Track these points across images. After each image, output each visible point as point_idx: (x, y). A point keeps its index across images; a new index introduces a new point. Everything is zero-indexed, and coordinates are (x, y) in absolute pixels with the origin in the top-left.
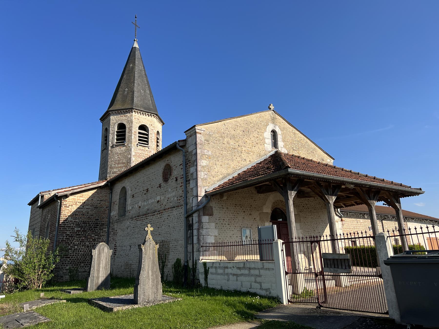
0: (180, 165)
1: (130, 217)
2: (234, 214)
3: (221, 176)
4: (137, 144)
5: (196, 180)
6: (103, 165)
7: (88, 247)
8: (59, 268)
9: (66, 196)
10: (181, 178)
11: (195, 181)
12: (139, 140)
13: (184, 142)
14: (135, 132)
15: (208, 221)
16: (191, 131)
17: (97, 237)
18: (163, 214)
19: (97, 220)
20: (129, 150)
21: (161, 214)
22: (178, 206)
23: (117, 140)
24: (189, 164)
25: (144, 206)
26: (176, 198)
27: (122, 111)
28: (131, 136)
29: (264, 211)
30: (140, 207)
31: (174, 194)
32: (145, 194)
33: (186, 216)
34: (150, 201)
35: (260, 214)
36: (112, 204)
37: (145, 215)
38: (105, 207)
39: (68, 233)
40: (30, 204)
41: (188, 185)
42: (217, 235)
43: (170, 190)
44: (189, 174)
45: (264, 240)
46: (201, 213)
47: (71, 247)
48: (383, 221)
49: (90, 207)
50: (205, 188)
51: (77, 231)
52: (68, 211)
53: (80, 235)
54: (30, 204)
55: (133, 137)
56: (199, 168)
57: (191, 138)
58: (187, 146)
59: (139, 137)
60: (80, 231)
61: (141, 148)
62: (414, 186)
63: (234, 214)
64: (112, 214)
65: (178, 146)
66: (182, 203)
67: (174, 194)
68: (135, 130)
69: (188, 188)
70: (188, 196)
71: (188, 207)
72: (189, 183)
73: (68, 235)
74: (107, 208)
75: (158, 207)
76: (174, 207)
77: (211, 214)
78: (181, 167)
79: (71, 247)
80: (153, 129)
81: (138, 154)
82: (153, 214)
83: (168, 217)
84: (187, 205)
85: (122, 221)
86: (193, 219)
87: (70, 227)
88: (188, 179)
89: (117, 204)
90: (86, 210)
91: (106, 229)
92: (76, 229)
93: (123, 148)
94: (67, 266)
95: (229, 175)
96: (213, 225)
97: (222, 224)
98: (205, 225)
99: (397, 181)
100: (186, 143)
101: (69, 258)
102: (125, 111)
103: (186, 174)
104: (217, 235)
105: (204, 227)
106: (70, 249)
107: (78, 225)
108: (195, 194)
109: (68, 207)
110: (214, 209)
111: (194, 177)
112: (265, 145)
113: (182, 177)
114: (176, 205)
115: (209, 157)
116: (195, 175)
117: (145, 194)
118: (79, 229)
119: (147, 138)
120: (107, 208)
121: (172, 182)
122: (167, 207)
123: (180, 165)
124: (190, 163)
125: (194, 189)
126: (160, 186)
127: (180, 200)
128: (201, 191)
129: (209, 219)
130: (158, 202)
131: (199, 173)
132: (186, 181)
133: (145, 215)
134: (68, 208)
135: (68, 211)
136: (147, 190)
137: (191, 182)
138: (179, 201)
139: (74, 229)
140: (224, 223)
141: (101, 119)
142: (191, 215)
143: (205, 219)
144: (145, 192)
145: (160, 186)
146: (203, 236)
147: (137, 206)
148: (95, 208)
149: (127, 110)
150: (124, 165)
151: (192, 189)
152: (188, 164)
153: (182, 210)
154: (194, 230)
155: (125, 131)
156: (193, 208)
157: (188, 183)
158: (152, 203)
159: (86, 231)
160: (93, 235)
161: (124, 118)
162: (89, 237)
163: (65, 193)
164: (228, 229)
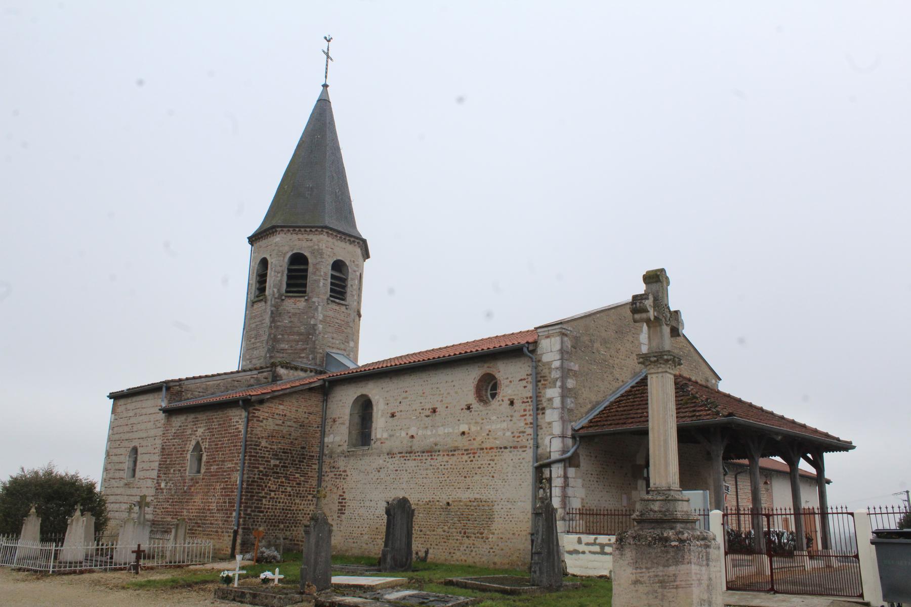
0: (521, 380)
1: (385, 451)
3: (589, 406)
4: (328, 299)
6: (253, 333)
7: (290, 496)
8: (249, 529)
9: (261, 402)
10: (523, 402)
12: (332, 290)
14: (326, 274)
17: (302, 479)
18: (476, 456)
19: (303, 448)
21: (472, 455)
22: (515, 447)
23: (288, 285)
24: (543, 382)
26: (508, 434)
28: (318, 281)
30: (412, 437)
31: (504, 425)
32: (427, 416)
34: (441, 431)
36: (329, 421)
39: (261, 469)
41: (539, 417)
42: (584, 497)
43: (494, 418)
44: (544, 400)
46: (567, 465)
49: (294, 425)
51: (275, 465)
53: (278, 473)
55: (321, 284)
57: (548, 340)
58: (539, 352)
59: (332, 284)
61: (334, 306)
62: (843, 437)
64: (326, 440)
65: (525, 350)
67: (504, 425)
68: (326, 269)
71: (540, 451)
72: (543, 413)
75: (462, 442)
76: (506, 448)
77: (577, 466)
78: (524, 383)
84: (537, 447)
85: (363, 455)
88: (540, 407)
89: (343, 424)
90: (287, 429)
91: (316, 467)
92: (273, 462)
93: (301, 304)
94: (260, 526)
95: (598, 403)
98: (571, 482)
99: (811, 423)
101: (262, 512)
104: (584, 497)
106: (263, 497)
114: (511, 445)
117: (427, 416)
118: (277, 462)
119: (344, 287)
121: (499, 405)
122: (484, 446)
123: (521, 380)
126: (469, 408)
130: (463, 433)
132: (538, 409)
137: (548, 412)
143: (571, 471)
144: (428, 413)
147: (403, 434)
150: (301, 337)
151: (549, 423)
152: (540, 381)
153: (529, 455)
154: (553, 489)
157: (540, 412)
158: (449, 434)
160: (297, 475)
161: (305, 244)
163: (262, 397)
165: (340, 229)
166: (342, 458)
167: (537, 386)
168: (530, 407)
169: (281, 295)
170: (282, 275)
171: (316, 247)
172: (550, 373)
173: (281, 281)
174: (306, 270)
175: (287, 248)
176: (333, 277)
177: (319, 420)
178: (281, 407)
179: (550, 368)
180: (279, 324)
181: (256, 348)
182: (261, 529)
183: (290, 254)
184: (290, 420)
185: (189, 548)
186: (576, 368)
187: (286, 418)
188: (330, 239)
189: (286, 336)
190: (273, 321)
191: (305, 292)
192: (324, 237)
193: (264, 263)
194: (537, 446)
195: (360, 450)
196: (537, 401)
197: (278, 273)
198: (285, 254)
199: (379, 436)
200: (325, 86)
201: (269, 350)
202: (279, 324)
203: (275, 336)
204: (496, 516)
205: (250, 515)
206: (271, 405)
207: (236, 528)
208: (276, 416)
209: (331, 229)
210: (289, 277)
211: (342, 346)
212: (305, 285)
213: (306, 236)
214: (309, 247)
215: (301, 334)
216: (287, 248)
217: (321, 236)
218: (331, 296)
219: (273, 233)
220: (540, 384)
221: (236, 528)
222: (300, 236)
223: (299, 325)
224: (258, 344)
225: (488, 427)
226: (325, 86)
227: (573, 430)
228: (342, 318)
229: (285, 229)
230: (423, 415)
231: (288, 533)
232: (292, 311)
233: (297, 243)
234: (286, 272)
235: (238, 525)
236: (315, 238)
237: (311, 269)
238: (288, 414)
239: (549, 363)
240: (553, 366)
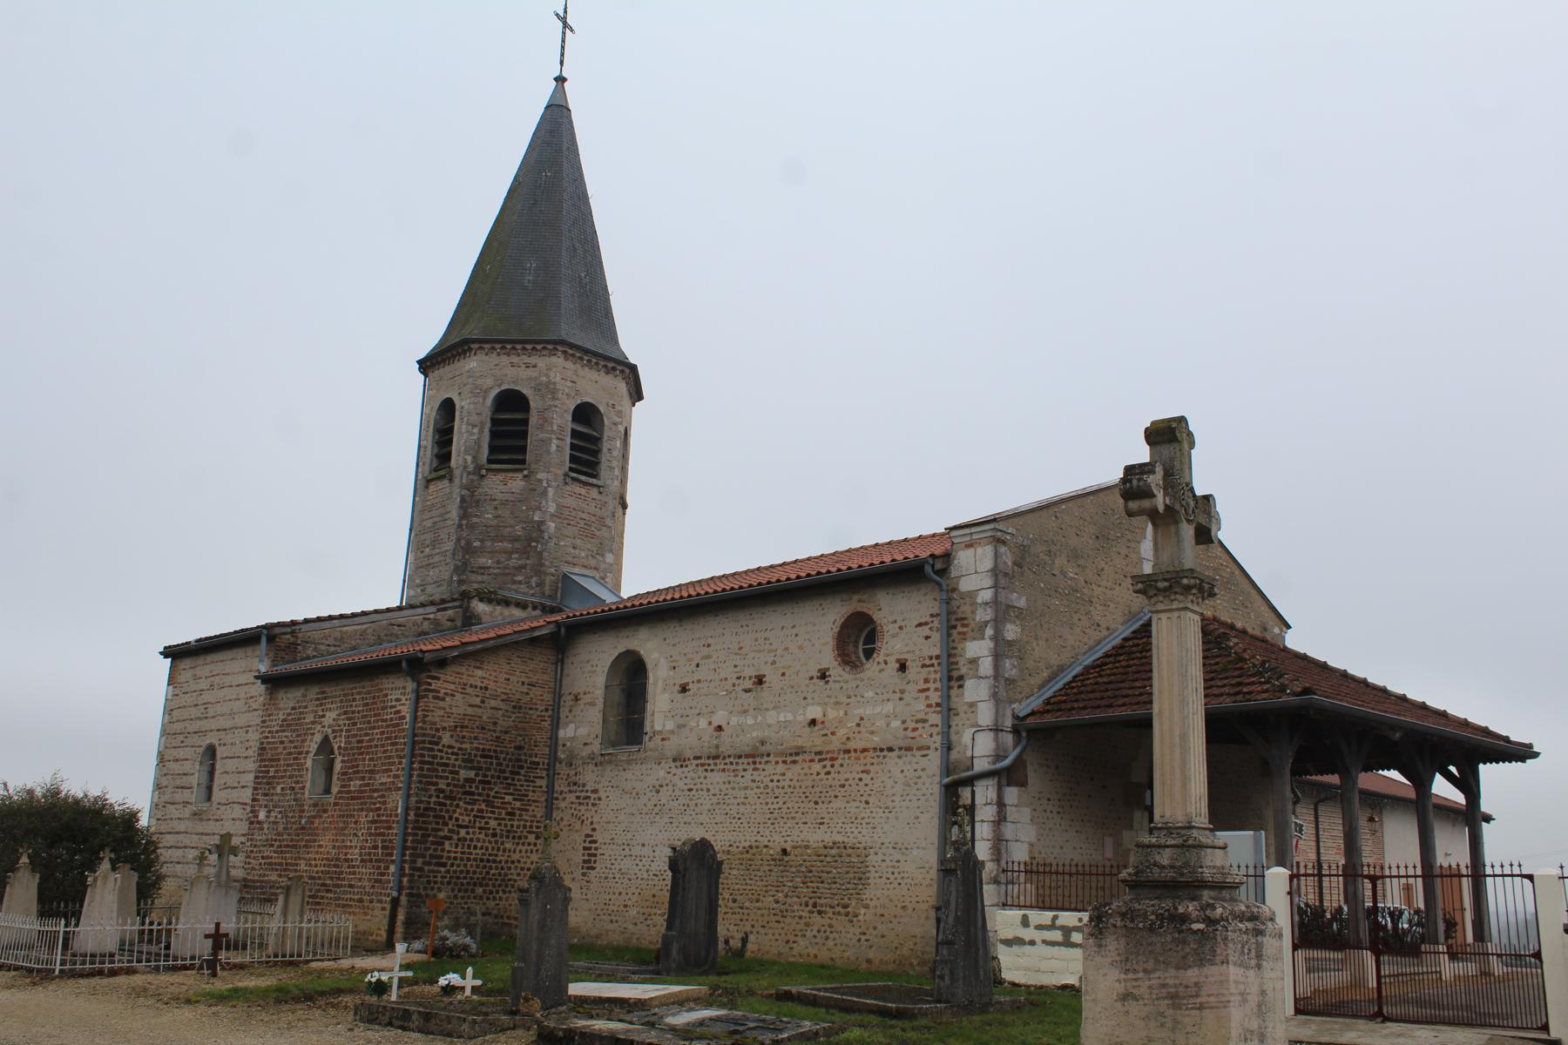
0: (920, 625)
1: (669, 754)
3: (1045, 674)
4: (566, 475)
6: (429, 537)
7: (494, 835)
8: (419, 895)
9: (442, 663)
10: (924, 666)
12: (573, 459)
16: (973, 530)
17: (518, 804)
18: (837, 763)
19: (520, 748)
20: (535, 491)
21: (828, 763)
22: (908, 749)
23: (492, 449)
24: (960, 629)
25: (742, 729)
26: (896, 724)
27: (519, 347)
28: (547, 442)
30: (720, 728)
31: (889, 707)
32: (747, 691)
34: (772, 718)
36: (567, 700)
37: (753, 756)
39: (442, 785)
40: (168, 652)
41: (953, 692)
42: (1034, 840)
43: (871, 694)
44: (962, 662)
46: (1004, 782)
47: (450, 831)
48: (1320, 808)
49: (502, 705)
51: (467, 780)
52: (441, 713)
53: (472, 794)
54: (168, 652)
55: (553, 448)
57: (971, 550)
59: (573, 447)
60: (473, 781)
61: (578, 489)
64: (561, 733)
65: (928, 569)
69: (954, 699)
70: (953, 723)
71: (954, 755)
72: (961, 686)
73: (443, 791)
75: (811, 740)
76: (890, 749)
77: (1022, 784)
78: (925, 631)
79: (450, 831)
82: (789, 759)
83: (864, 776)
84: (949, 749)
85: (629, 762)
87: (447, 765)
88: (955, 674)
89: (592, 704)
91: (543, 783)
92: (463, 774)
93: (516, 483)
94: (439, 890)
95: (1062, 669)
98: (1011, 813)
101: (444, 865)
102: (529, 347)
103: (949, 656)
104: (1034, 840)
106: (446, 838)
107: (468, 762)
113: (928, 662)
117: (747, 691)
118: (472, 774)
119: (596, 453)
121: (879, 671)
122: (851, 745)
123: (920, 625)
126: (823, 676)
127: (915, 729)
129: (1019, 796)
130: (813, 722)
132: (950, 679)
133: (753, 756)
134: (441, 704)
135: (441, 713)
136: (760, 680)
137: (969, 684)
139: (457, 773)
143: (1012, 794)
144: (748, 684)
145: (823, 676)
147: (703, 723)
150: (517, 545)
151: (972, 705)
152: (954, 627)
153: (934, 761)
154: (977, 825)
157: (954, 683)
159: (488, 783)
160: (508, 798)
161: (523, 373)
162: (497, 802)
163: (444, 654)
165: (588, 345)
166: (591, 767)
167: (949, 635)
168: (935, 674)
169: (478, 468)
170: (481, 431)
171: (544, 379)
172: (973, 612)
173: (478, 442)
174: (526, 422)
175: (489, 382)
176: (575, 434)
177: (548, 697)
178: (479, 673)
179: (974, 604)
180: (475, 520)
182: (442, 895)
183: (497, 391)
184: (495, 697)
185: (253, 929)
186: (1022, 603)
188: (569, 364)
190: (465, 515)
191: (523, 462)
192: (559, 360)
193: (448, 408)
194: (948, 747)
195: (623, 753)
196: (950, 664)
197: (474, 426)
198: (487, 391)
199: (658, 727)
200: (561, 80)
201: (456, 568)
202: (475, 520)
203: (469, 543)
205: (420, 869)
206: (460, 669)
207: (395, 894)
208: (469, 690)
209: (572, 346)
210: (493, 434)
211: (592, 562)
212: (523, 450)
213: (526, 359)
215: (515, 539)
216: (489, 382)
217: (554, 359)
218: (571, 469)
219: (465, 352)
220: (954, 632)
221: (395, 894)
222: (515, 359)
224: (436, 559)
225: (859, 711)
226: (561, 80)
227: (1015, 717)
228: (592, 510)
229: (487, 346)
231: (491, 904)
233: (510, 371)
234: (488, 425)
235: (400, 889)
236: (542, 362)
237: (534, 420)
238: (492, 685)
239: (972, 595)
240: (979, 600)
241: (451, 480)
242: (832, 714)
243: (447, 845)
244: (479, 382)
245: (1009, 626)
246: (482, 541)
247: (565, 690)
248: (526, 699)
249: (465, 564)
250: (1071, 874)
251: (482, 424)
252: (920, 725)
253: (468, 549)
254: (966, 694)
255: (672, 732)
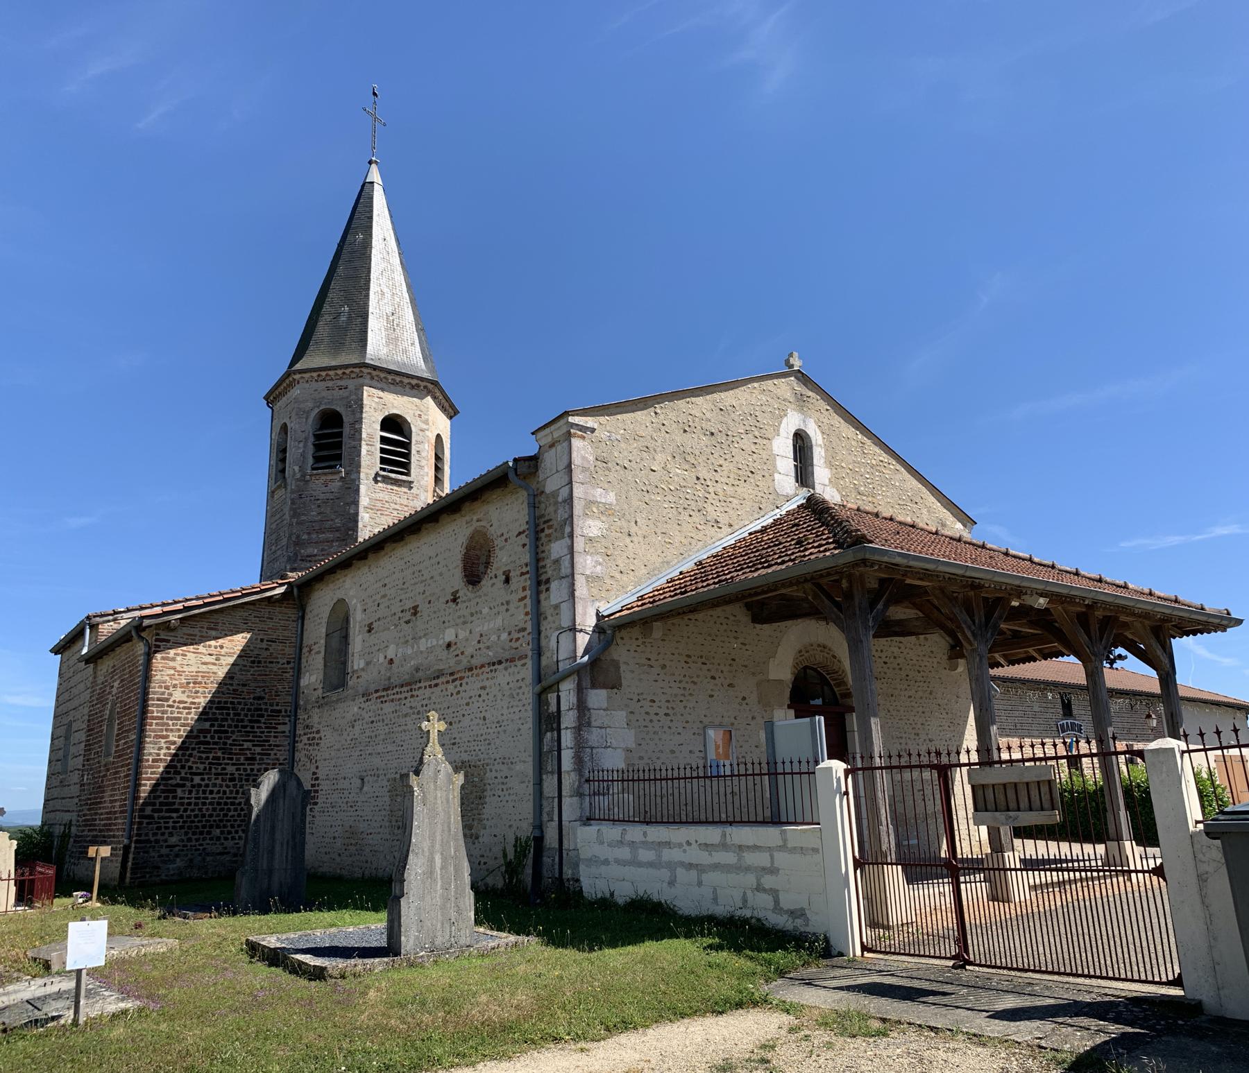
0: (520, 534)
1: (361, 690)
2: (682, 685)
4: (377, 475)
5: (569, 579)
6: (274, 536)
8: (148, 841)
10: (522, 574)
11: (565, 583)
12: (383, 461)
13: (532, 463)
14: (370, 436)
15: (605, 705)
16: (553, 427)
17: (258, 750)
18: (464, 682)
20: (352, 489)
21: (458, 683)
22: (512, 660)
23: (317, 459)
24: (547, 532)
26: (504, 636)
29: (771, 677)
30: (391, 661)
33: (538, 688)
34: (423, 644)
35: (758, 684)
36: (305, 650)
37: (408, 684)
38: (281, 661)
40: (56, 651)
41: (542, 597)
42: (632, 745)
43: (486, 610)
44: (548, 562)
45: (787, 761)
46: (587, 682)
47: (182, 779)
50: (597, 604)
53: (208, 743)
54: (56, 651)
56: (579, 544)
57: (553, 450)
58: (541, 476)
59: (382, 451)
60: (208, 731)
62: (1213, 605)
63: (682, 685)
64: (304, 682)
66: (527, 649)
67: (499, 622)
68: (371, 430)
69: (543, 603)
70: (543, 628)
71: (544, 662)
72: (548, 590)
74: (288, 663)
75: (447, 661)
76: (500, 662)
77: (615, 685)
79: (182, 779)
80: (425, 427)
81: (379, 504)
82: (433, 682)
83: (482, 692)
85: (338, 701)
86: (559, 698)
87: (179, 719)
88: (544, 578)
89: (319, 652)
91: (286, 728)
94: (171, 834)
96: (620, 716)
97: (647, 713)
98: (597, 718)
100: (536, 468)
101: (177, 811)
103: (538, 560)
104: (632, 745)
105: (594, 724)
106: (178, 785)
108: (566, 623)
109: (173, 659)
110: (623, 667)
111: (565, 570)
112: (776, 476)
113: (525, 570)
114: (507, 655)
115: (607, 511)
116: (566, 563)
119: (407, 456)
120: (288, 663)
121: (491, 586)
122: (475, 662)
123: (520, 534)
124: (550, 527)
125: (564, 607)
127: (518, 639)
128: (585, 614)
129: (609, 698)
130: (449, 645)
131: (578, 559)
132: (539, 583)
133: (408, 684)
134: (171, 664)
135: (172, 672)
136: (415, 611)
137: (554, 585)
138: (514, 645)
140: (652, 711)
141: (266, 398)
142: (554, 687)
143: (597, 698)
144: (408, 616)
146: (592, 748)
147: (381, 659)
148: (253, 662)
149: (347, 371)
151: (557, 607)
152: (543, 530)
154: (563, 732)
155: (340, 435)
156: (561, 664)
157: (543, 587)
158: (430, 650)
159: (226, 732)
160: (246, 745)
162: (236, 749)
164: (666, 729)
166: (317, 710)
167: (537, 539)
169: (304, 475)
170: (305, 446)
172: (556, 511)
173: (303, 455)
175: (310, 405)
176: (384, 440)
177: (289, 650)
179: (556, 503)
180: (303, 518)
181: (275, 560)
182: (173, 840)
183: (316, 411)
186: (611, 498)
187: (223, 651)
189: (314, 536)
190: (295, 514)
191: (409, 485)
193: (284, 428)
194: (539, 652)
195: (333, 696)
198: (308, 413)
199: (356, 668)
201: (289, 558)
202: (303, 518)
203: (298, 537)
204: (488, 793)
205: (151, 817)
207: (126, 841)
210: (318, 447)
214: (341, 399)
220: (543, 535)
221: (126, 841)
223: (333, 517)
224: (279, 553)
227: (599, 617)
230: (402, 621)
231: (229, 843)
232: (322, 496)
233: (325, 394)
234: (312, 439)
235: (130, 838)
237: (346, 430)
239: (555, 494)
240: (560, 499)
241: (285, 487)
242: (463, 634)
243: (179, 790)
244: (302, 406)
245: (590, 522)
246: (309, 534)
247: (305, 643)
248: (266, 654)
249: (296, 554)
250: (623, 781)
251: (306, 439)
252: (520, 635)
253: (298, 543)
254: (552, 597)
255: (363, 669)
